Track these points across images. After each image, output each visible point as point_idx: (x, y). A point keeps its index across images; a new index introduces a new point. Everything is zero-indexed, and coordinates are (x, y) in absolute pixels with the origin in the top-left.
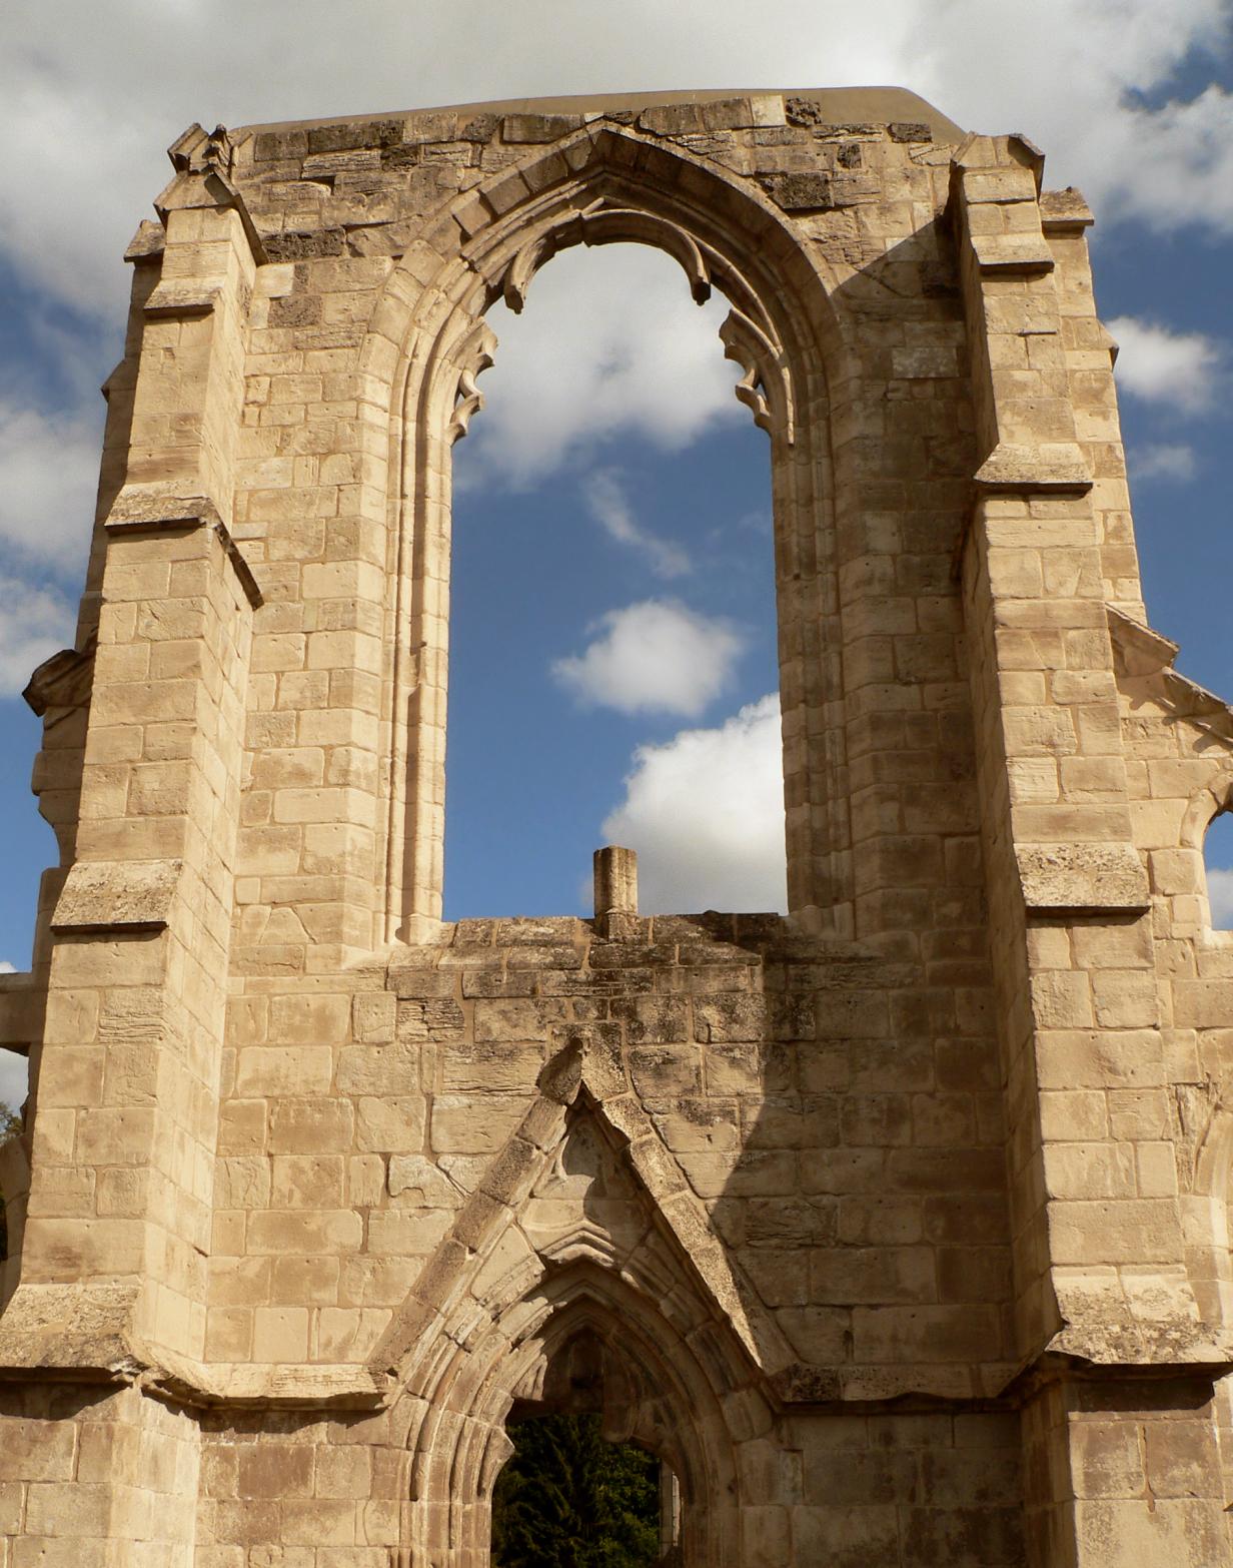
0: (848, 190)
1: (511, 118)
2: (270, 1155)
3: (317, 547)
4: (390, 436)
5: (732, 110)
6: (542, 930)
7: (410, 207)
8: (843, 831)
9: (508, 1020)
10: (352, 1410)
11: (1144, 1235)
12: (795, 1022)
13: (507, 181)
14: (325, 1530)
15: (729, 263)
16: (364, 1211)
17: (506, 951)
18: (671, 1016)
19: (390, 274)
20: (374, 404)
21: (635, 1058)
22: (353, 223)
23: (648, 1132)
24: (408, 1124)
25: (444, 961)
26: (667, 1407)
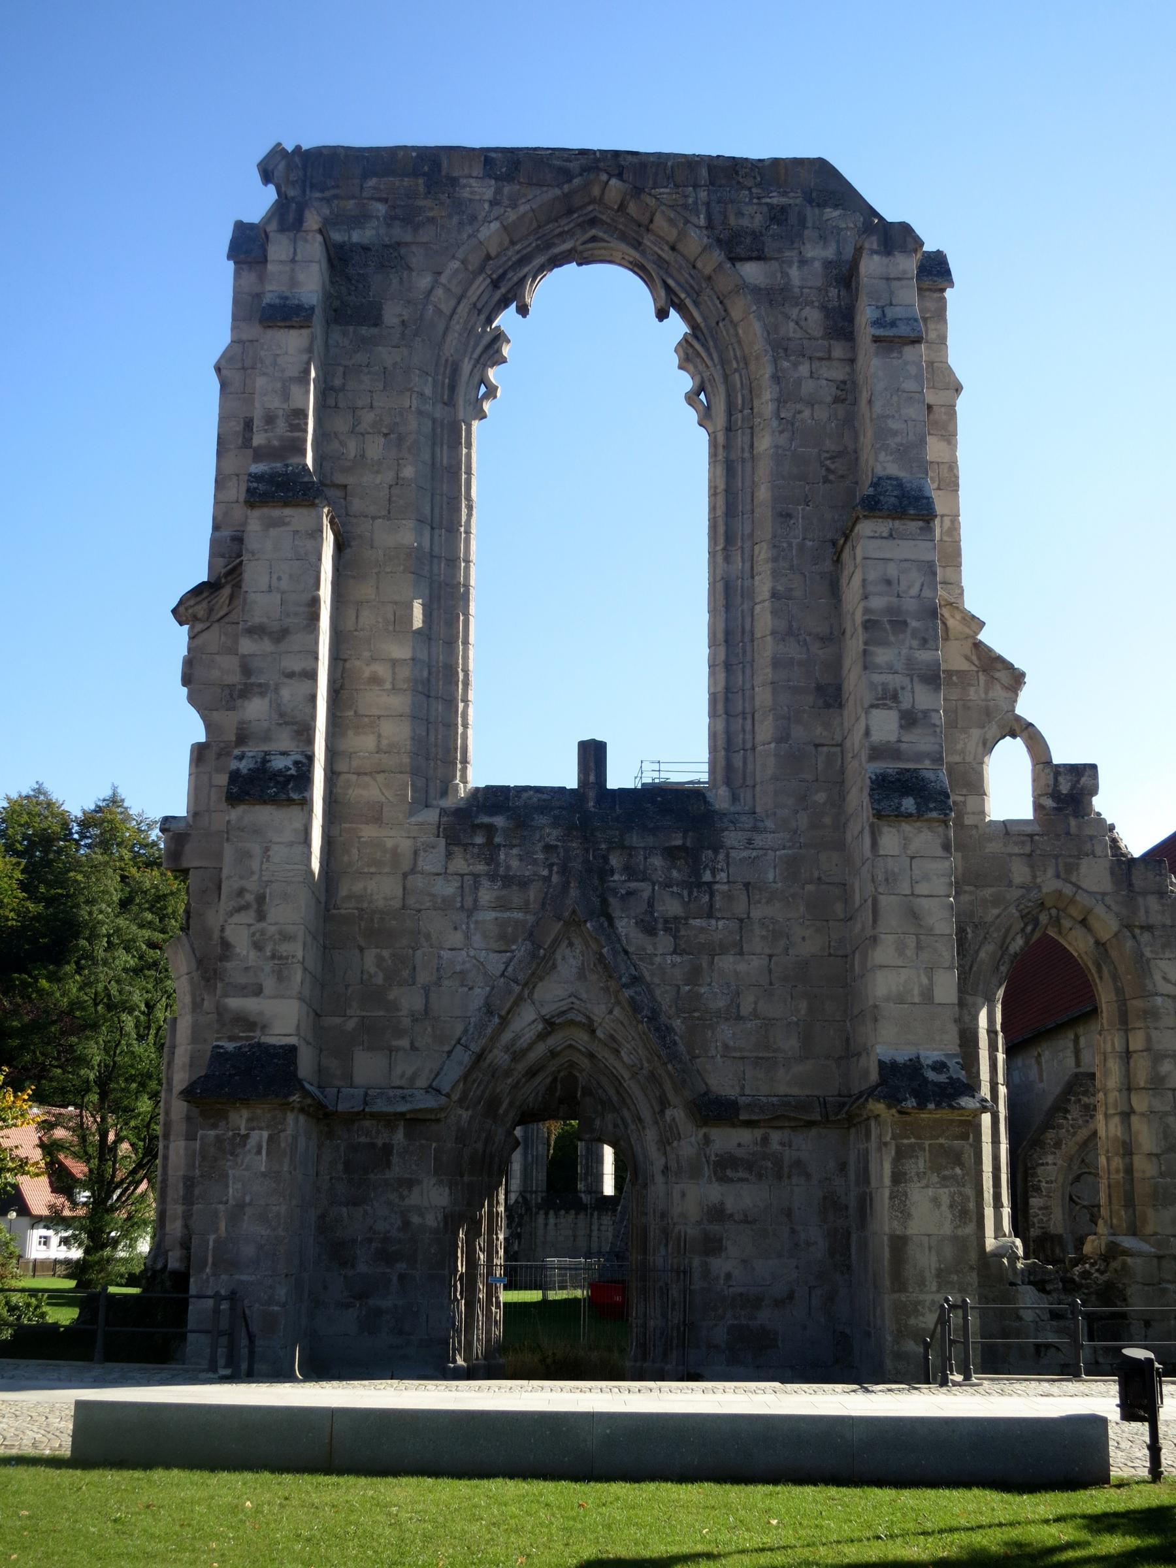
22: (403, 241)
26: (623, 1119)
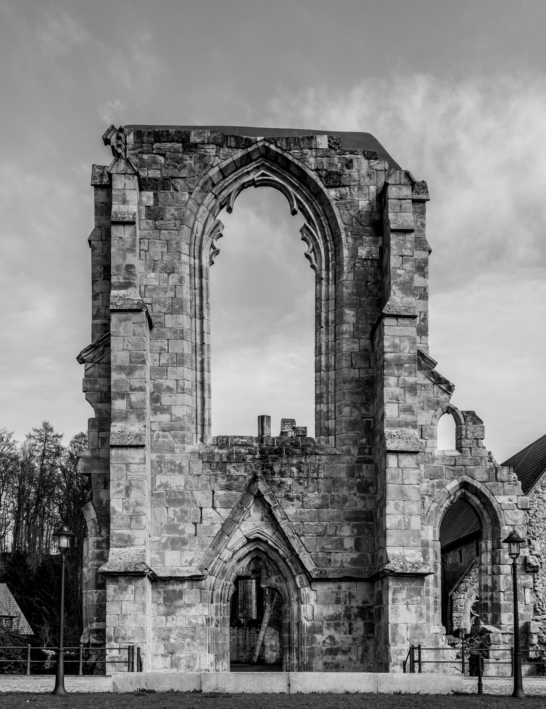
0: (347, 179)
1: (230, 137)
2: (167, 508)
3: (169, 309)
4: (190, 265)
5: (309, 140)
6: (243, 440)
7: (194, 172)
8: (333, 414)
9: (236, 469)
10: (195, 579)
11: (411, 539)
12: (318, 473)
13: (229, 164)
14: (188, 612)
15: (305, 204)
16: (195, 524)
17: (234, 447)
18: (283, 469)
19: (188, 200)
20: (185, 254)
21: (273, 481)
23: (276, 503)
24: (207, 499)
25: (216, 451)
